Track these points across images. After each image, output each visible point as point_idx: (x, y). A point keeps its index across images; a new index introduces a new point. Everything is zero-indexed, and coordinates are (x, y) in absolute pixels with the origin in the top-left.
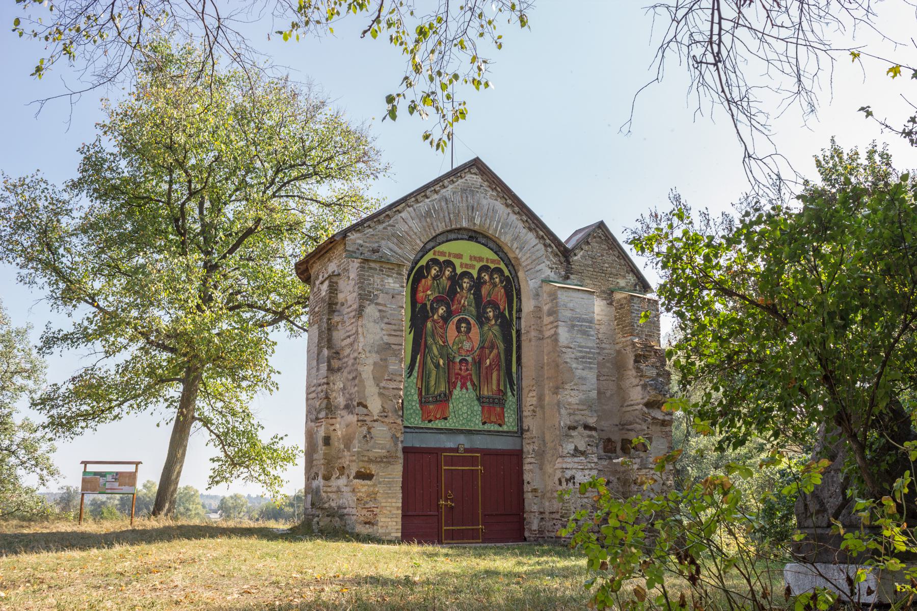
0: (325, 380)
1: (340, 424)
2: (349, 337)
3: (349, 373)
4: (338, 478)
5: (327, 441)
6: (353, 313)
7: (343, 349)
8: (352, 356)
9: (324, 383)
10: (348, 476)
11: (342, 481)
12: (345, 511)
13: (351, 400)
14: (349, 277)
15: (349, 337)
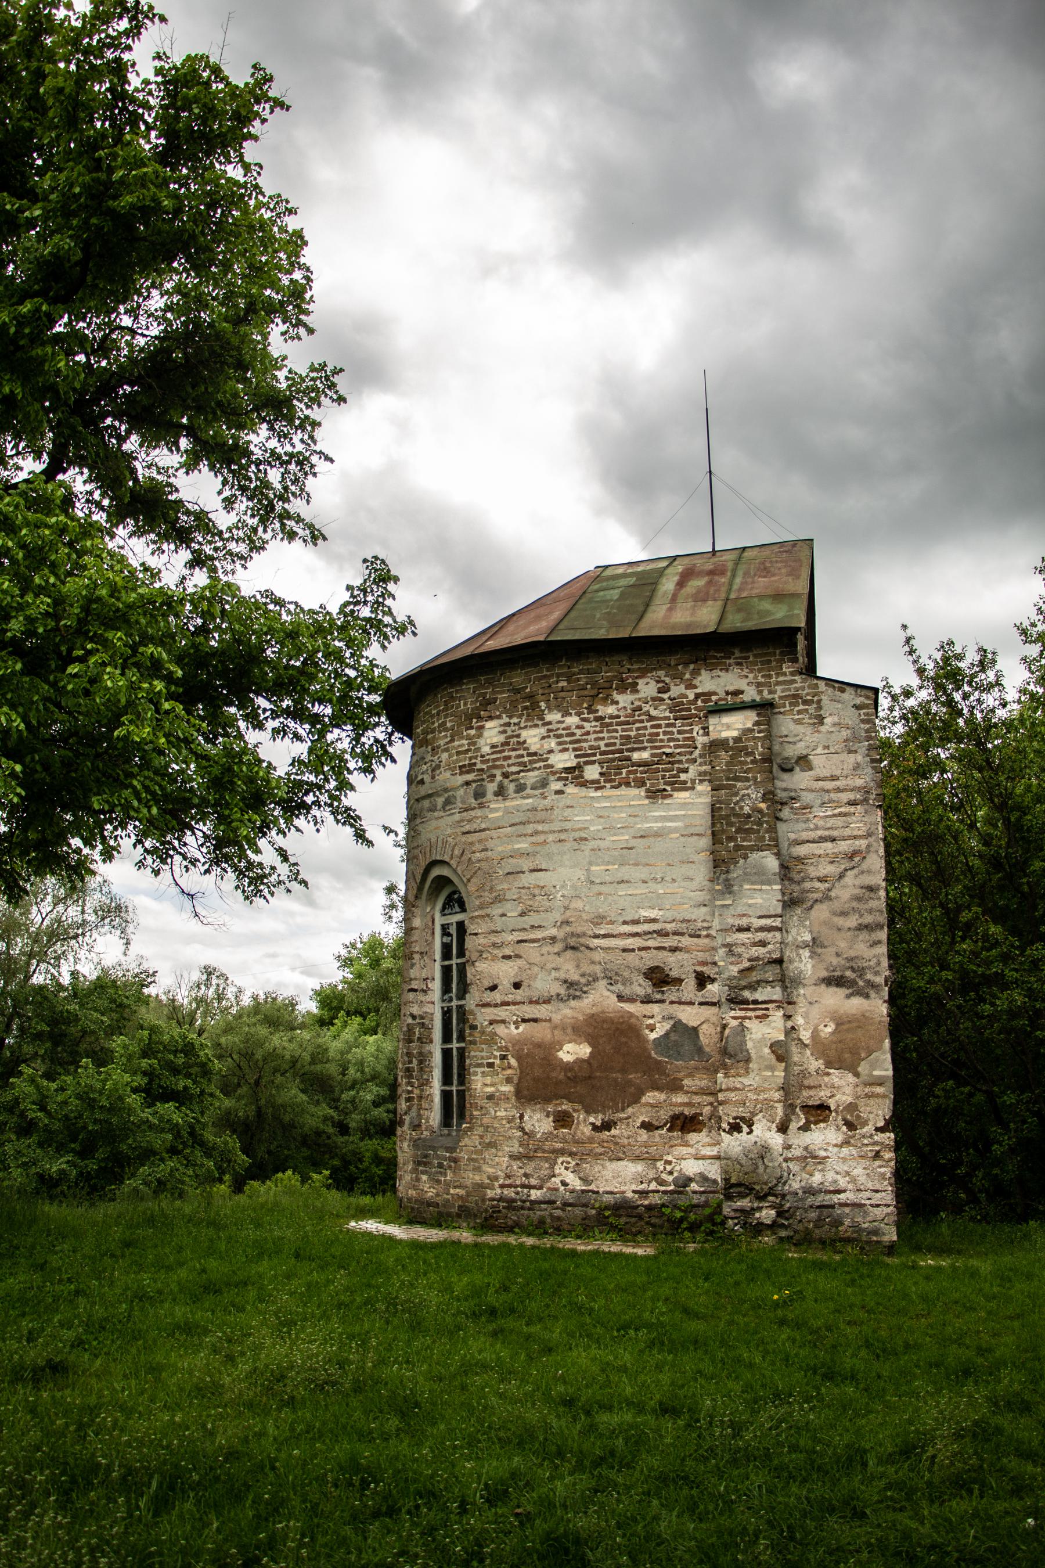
0: (777, 922)
1: (806, 1016)
2: (833, 840)
3: (844, 914)
4: (805, 1128)
5: (780, 1052)
6: (851, 796)
7: (800, 860)
8: (849, 878)
9: (762, 929)
10: (851, 1126)
11: (824, 1137)
12: (836, 1198)
13: (861, 972)
14: (821, 720)
15: (833, 840)
